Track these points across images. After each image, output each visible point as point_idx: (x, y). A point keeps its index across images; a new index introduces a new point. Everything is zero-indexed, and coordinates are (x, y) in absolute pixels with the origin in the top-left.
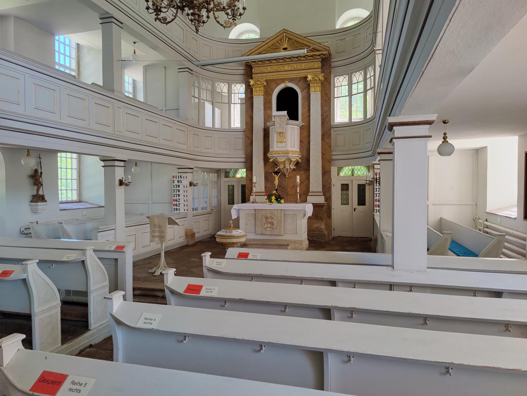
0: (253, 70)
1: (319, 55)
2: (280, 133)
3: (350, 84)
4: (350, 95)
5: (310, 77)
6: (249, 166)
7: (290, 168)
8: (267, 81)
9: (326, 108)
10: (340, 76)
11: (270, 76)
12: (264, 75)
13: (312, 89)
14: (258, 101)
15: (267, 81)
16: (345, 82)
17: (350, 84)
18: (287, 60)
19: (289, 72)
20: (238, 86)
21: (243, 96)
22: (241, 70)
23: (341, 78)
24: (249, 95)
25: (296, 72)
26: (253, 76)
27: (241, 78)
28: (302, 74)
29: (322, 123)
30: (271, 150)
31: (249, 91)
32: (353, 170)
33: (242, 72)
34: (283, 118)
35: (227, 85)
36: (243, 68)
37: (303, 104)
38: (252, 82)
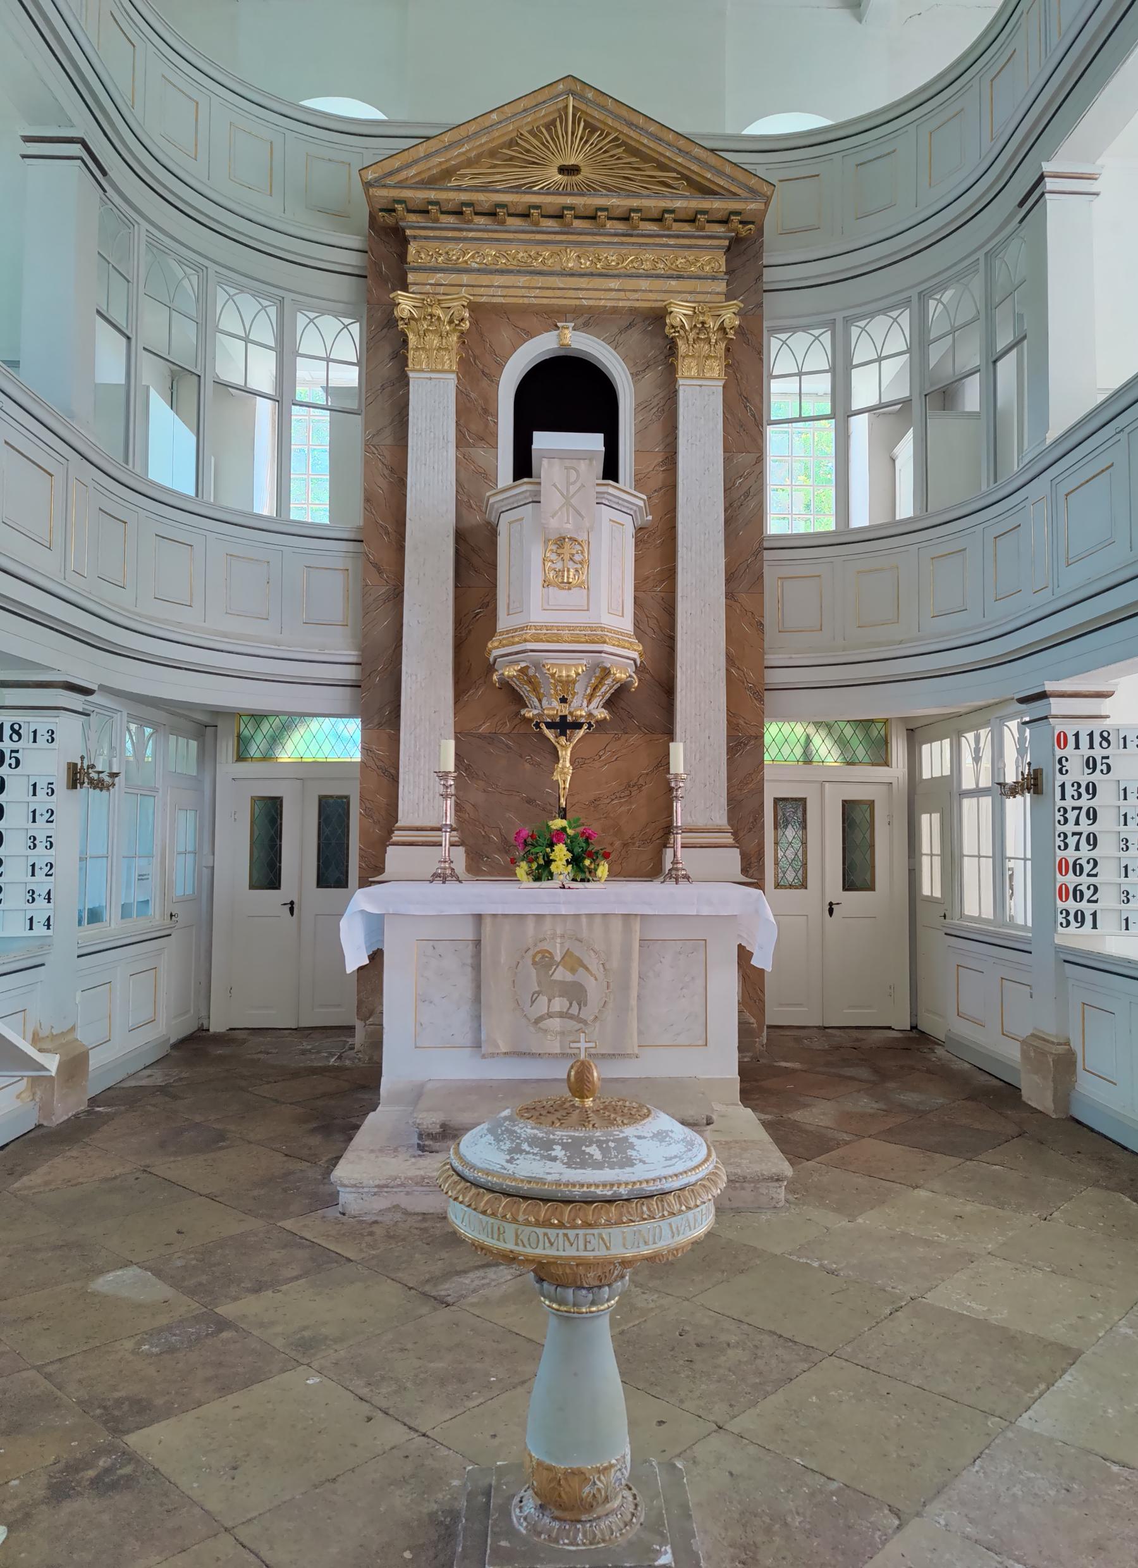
0: (412, 249)
1: (725, 222)
2: (560, 541)
3: (841, 371)
4: (842, 410)
5: (680, 312)
6: (377, 697)
7: (590, 715)
8: (473, 307)
9: (740, 458)
10: (794, 329)
11: (497, 290)
12: (465, 279)
13: (687, 368)
14: (433, 398)
15: (473, 307)
16: (819, 359)
17: (841, 371)
18: (577, 223)
19: (583, 282)
20: (330, 324)
21: (349, 377)
22: (345, 246)
23: (800, 340)
24: (387, 368)
25: (614, 284)
26: (411, 277)
27: (343, 288)
28: (643, 294)
29: (727, 522)
30: (504, 622)
31: (386, 350)
32: (808, 740)
33: (352, 260)
34: (583, 466)
35: (273, 311)
36: (355, 241)
37: (640, 432)
38: (405, 304)
